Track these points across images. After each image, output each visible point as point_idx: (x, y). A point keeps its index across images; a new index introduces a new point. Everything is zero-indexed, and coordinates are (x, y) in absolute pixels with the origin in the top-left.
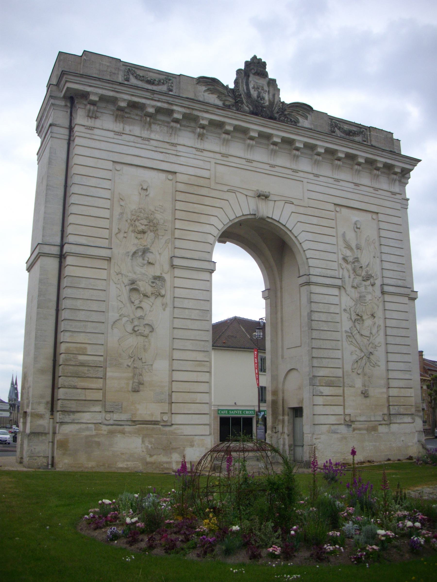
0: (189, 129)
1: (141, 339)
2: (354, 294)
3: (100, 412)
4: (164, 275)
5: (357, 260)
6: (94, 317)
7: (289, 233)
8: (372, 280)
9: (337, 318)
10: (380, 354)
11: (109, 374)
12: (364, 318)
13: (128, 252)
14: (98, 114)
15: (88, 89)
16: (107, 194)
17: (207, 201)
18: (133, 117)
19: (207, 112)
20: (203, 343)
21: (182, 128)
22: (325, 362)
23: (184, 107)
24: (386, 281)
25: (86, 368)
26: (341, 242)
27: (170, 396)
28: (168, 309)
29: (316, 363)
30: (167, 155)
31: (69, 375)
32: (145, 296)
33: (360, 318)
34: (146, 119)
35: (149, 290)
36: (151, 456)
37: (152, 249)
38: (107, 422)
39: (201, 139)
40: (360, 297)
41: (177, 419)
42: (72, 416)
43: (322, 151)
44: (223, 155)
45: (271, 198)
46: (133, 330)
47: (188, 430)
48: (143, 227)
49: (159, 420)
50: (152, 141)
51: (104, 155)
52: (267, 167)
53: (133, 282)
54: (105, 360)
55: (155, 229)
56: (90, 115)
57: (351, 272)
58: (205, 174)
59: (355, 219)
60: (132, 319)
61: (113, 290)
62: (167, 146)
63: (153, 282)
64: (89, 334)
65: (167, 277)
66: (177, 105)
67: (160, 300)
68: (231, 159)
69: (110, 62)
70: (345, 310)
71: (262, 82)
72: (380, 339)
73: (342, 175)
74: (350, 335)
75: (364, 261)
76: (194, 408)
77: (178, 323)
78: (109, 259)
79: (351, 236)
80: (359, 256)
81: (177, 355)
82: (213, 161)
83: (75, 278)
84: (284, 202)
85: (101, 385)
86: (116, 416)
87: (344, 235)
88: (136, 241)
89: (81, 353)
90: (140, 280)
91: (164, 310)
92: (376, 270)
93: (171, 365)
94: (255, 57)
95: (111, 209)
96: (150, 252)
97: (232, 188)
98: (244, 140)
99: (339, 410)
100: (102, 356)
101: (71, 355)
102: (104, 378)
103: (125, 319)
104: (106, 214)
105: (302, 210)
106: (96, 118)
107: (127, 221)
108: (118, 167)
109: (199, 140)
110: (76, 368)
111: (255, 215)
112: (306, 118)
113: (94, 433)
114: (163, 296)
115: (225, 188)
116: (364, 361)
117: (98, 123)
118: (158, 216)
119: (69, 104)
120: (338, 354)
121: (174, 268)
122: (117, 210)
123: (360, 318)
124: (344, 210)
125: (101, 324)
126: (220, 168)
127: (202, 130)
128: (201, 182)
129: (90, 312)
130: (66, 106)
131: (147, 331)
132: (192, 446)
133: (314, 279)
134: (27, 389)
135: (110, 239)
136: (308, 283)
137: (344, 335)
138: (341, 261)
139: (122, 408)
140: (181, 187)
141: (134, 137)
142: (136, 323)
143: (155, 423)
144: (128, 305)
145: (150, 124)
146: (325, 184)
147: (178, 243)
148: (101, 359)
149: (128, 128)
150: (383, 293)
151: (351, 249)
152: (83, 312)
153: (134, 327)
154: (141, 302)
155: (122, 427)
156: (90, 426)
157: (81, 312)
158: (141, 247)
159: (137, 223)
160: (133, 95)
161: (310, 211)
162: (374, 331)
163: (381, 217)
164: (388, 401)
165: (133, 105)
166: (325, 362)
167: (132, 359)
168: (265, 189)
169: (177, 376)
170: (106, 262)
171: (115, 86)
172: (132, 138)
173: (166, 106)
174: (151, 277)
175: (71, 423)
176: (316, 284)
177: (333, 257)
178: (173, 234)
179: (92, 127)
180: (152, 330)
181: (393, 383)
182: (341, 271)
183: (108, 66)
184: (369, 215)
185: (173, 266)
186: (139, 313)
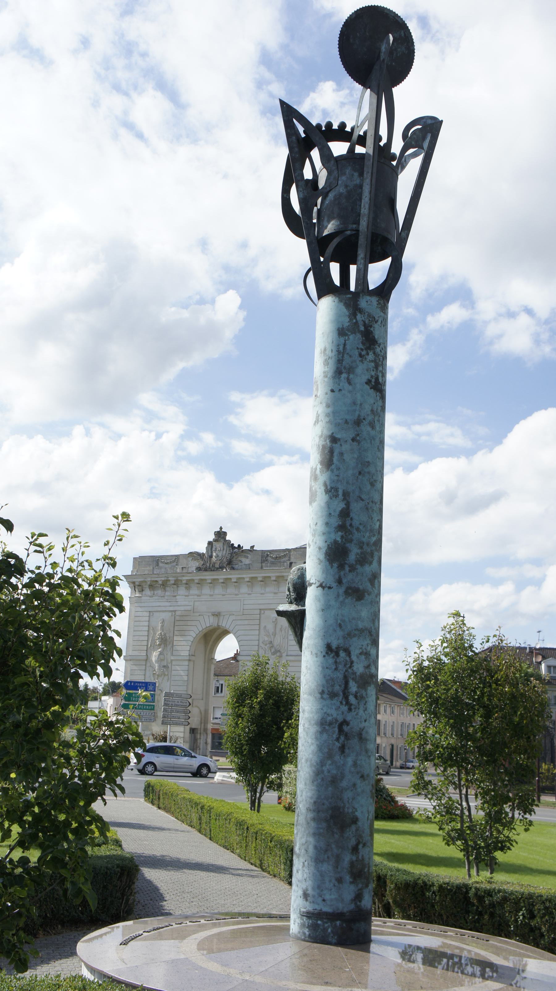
8: (278, 654)
65: (170, 665)
67: (166, 678)
75: (276, 643)
87: (265, 627)
94: (221, 528)
112: (247, 557)
124: (266, 612)
126: (197, 604)
140: (177, 618)
172: (157, 597)
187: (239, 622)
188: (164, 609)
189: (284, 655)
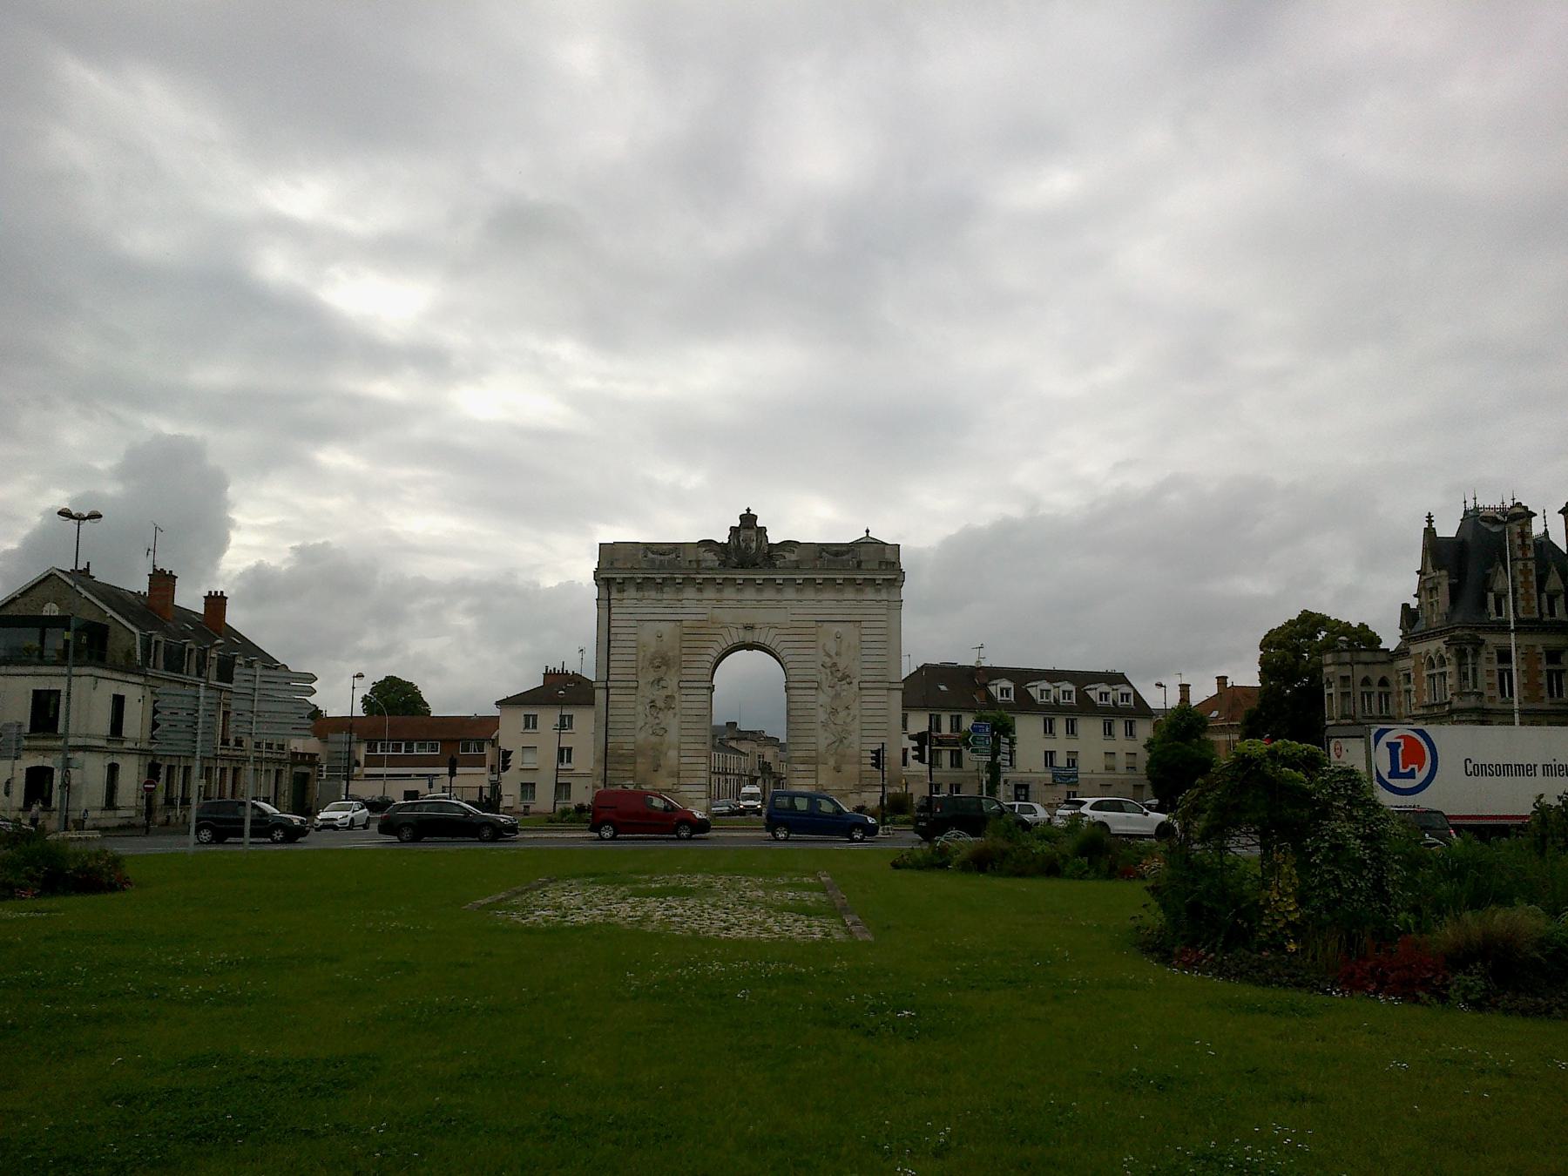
2: (831, 692)
5: (835, 664)
9: (813, 712)
14: (625, 588)
15: (614, 576)
16: (633, 644)
17: (706, 638)
22: (801, 747)
26: (821, 653)
33: (834, 712)
41: (683, 788)
45: (757, 626)
47: (690, 795)
51: (632, 617)
58: (704, 617)
61: (640, 708)
62: (676, 602)
65: (677, 695)
70: (821, 706)
71: (752, 533)
72: (856, 725)
73: (826, 596)
74: (824, 725)
76: (695, 781)
81: (683, 746)
88: (655, 674)
93: (679, 753)
94: (748, 510)
98: (735, 586)
99: (813, 781)
102: (635, 763)
104: (634, 658)
106: (624, 591)
108: (641, 623)
114: (673, 708)
117: (625, 595)
118: (670, 654)
120: (813, 740)
122: (642, 654)
123: (834, 712)
124: (825, 624)
128: (701, 624)
131: (662, 732)
140: (686, 630)
150: (860, 689)
151: (830, 656)
154: (658, 713)
159: (655, 662)
163: (864, 624)
164: (860, 775)
166: (801, 747)
169: (684, 760)
172: (649, 601)
177: (813, 665)
178: (680, 665)
180: (666, 731)
184: (852, 624)
186: (657, 721)
187: (783, 638)
189: (855, 682)
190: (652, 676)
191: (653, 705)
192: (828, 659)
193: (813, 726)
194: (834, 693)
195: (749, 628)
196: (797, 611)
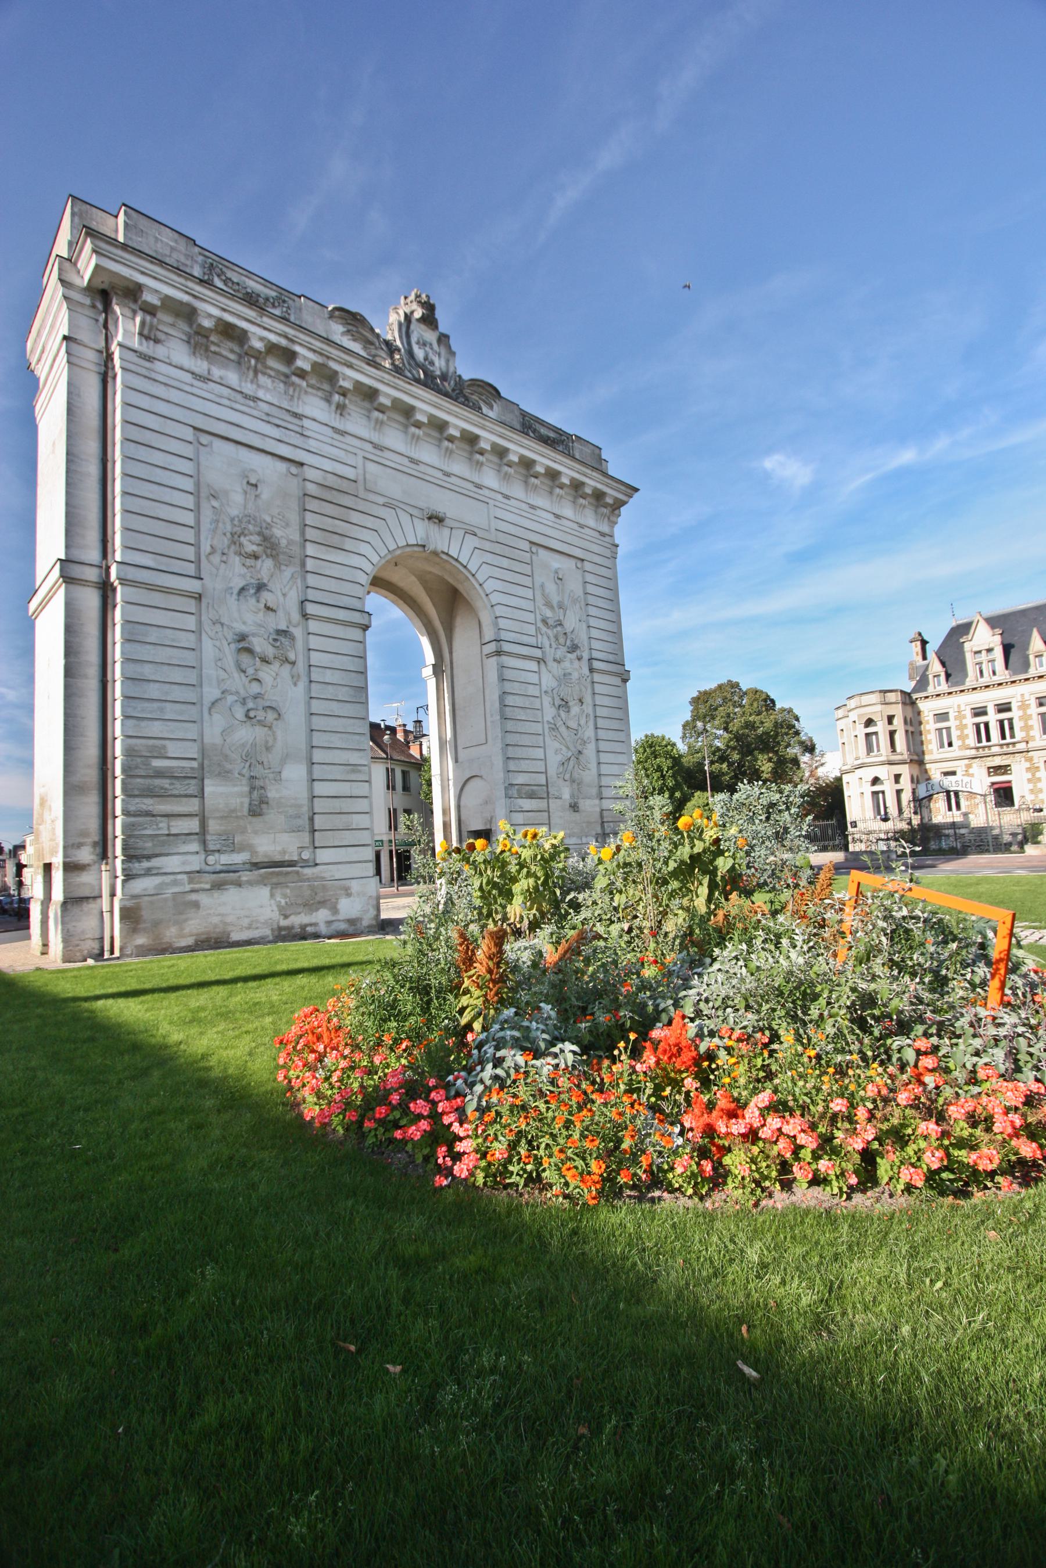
0: (320, 393)
1: (260, 732)
3: (197, 853)
4: (292, 629)
6: (177, 693)
7: (470, 577)
8: (578, 652)
10: (590, 750)
11: (207, 790)
12: (570, 704)
13: (231, 588)
17: (355, 517)
18: (225, 353)
19: (350, 366)
20: (357, 737)
21: (310, 390)
22: (524, 765)
23: (314, 351)
24: (595, 654)
25: (168, 781)
27: (311, 820)
28: (302, 684)
29: (512, 766)
30: (287, 432)
31: (137, 793)
32: (265, 660)
34: (249, 361)
35: (270, 652)
36: (286, 917)
37: (271, 586)
38: (208, 868)
39: (341, 415)
40: (565, 675)
42: (146, 864)
43: (516, 459)
44: (376, 446)
45: (447, 522)
46: (247, 716)
48: (255, 548)
49: (296, 858)
50: (260, 403)
52: (439, 475)
53: (242, 638)
54: (202, 766)
55: (274, 552)
56: (146, 332)
57: (553, 639)
58: (350, 473)
59: (555, 565)
60: (244, 699)
63: (275, 640)
64: (169, 723)
65: (298, 632)
66: (301, 344)
68: (387, 454)
69: (176, 241)
72: (590, 733)
76: (348, 838)
77: (317, 706)
78: (199, 597)
79: (551, 588)
80: (562, 618)
82: (361, 454)
83: (137, 626)
84: (463, 532)
85: (196, 808)
86: (225, 859)
87: (542, 586)
88: (244, 570)
89: (155, 754)
90: (254, 635)
91: (295, 684)
92: (582, 637)
93: (310, 772)
95: (197, 510)
96: (268, 590)
97: (390, 501)
100: (195, 759)
101: (139, 760)
102: (201, 795)
103: (230, 699)
105: (487, 546)
107: (225, 534)
108: (205, 439)
109: (338, 416)
110: (148, 781)
111: (424, 546)
112: (491, 407)
113: (188, 888)
115: (381, 500)
116: (571, 763)
117: (160, 351)
118: (278, 532)
119: (100, 306)
120: (539, 753)
121: (307, 619)
124: (541, 551)
125: (190, 707)
126: (371, 467)
127: (342, 398)
128: (345, 485)
129: (168, 686)
130: (94, 306)
131: (271, 716)
132: (349, 895)
133: (506, 647)
134: (49, 822)
135: (198, 562)
136: (499, 653)
137: (546, 726)
138: (540, 624)
139: (233, 843)
140: (311, 488)
141: (229, 391)
142: (250, 705)
143: (291, 864)
144: (236, 675)
145: (256, 372)
146: (517, 511)
147: (311, 580)
148: (195, 764)
149: (217, 372)
150: (592, 670)
152: (157, 685)
153: (248, 711)
155: (237, 874)
156: (179, 877)
157: (152, 684)
158: (253, 581)
160: (224, 310)
161: (498, 549)
162: (583, 722)
163: (588, 566)
164: (602, 817)
165: (228, 331)
166: (524, 765)
167: (248, 764)
168: (440, 509)
169: (320, 789)
170: (193, 602)
171: (190, 284)
172: (226, 392)
173: (284, 342)
174: (272, 631)
175: (144, 875)
176: (509, 654)
177: (530, 618)
178: (303, 564)
179: (150, 357)
181: (606, 793)
182: (540, 636)
183: (172, 249)
184: (573, 562)
185: (305, 616)
186: (255, 688)
187: (489, 558)
188: (257, 442)
190: (237, 573)
191: (243, 644)
192: (549, 613)
193: (537, 728)
194: (561, 672)
195: (436, 519)
196: (500, 514)
